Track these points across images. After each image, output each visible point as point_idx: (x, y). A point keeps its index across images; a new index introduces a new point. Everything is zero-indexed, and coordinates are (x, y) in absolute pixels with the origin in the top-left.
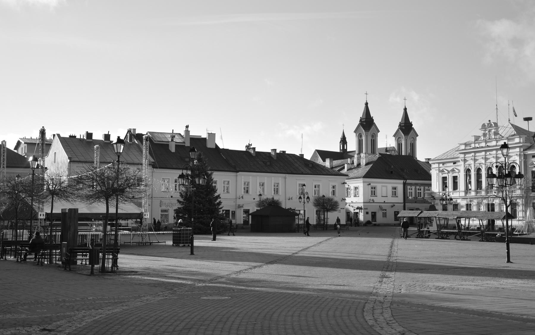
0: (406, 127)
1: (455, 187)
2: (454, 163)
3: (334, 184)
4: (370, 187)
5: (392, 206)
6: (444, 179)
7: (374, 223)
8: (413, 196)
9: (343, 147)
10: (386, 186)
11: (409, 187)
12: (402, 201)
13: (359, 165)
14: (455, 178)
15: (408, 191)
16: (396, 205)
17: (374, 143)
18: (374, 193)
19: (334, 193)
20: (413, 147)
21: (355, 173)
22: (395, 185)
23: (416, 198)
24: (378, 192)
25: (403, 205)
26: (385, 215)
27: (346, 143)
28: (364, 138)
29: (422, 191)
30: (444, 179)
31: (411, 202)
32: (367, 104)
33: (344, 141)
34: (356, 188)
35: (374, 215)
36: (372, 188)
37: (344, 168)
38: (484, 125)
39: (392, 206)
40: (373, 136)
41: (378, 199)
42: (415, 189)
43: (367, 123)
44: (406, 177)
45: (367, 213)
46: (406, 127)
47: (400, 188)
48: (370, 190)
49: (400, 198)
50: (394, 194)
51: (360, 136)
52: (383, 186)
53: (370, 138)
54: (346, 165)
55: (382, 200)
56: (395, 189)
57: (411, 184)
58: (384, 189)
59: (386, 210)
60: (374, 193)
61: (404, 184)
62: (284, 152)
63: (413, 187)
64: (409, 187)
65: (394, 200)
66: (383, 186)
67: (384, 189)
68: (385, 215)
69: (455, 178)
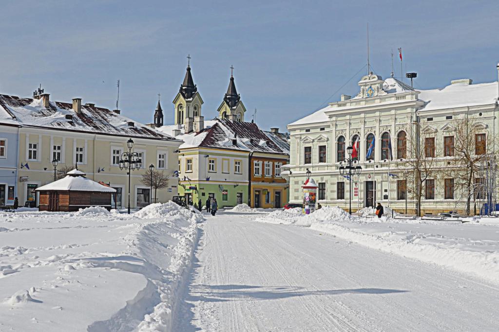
0: (233, 99)
1: (322, 159)
6: (308, 150)
11: (255, 162)
14: (322, 149)
15: (255, 167)
16: (240, 184)
19: (161, 164)
24: (218, 166)
25: (248, 184)
27: (162, 116)
29: (271, 168)
30: (308, 150)
31: (257, 180)
34: (189, 161)
36: (210, 162)
39: (235, 186)
40: (195, 108)
42: (263, 164)
43: (189, 90)
46: (233, 99)
48: (208, 164)
55: (222, 178)
57: (258, 158)
59: (227, 191)
63: (261, 162)
65: (237, 178)
66: (223, 159)
67: (226, 162)
69: (322, 149)
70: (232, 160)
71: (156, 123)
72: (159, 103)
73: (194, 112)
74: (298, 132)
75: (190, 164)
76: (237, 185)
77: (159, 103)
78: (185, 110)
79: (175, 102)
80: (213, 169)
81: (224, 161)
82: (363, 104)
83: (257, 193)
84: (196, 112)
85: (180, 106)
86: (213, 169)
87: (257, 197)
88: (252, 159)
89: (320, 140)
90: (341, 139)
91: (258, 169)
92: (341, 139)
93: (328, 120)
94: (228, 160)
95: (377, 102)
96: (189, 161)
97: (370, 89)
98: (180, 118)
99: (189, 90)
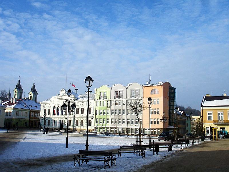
1: (49, 113)
6: (45, 110)
8: (33, 116)
10: (23, 112)
12: (29, 118)
13: (12, 103)
14: (49, 110)
23: (34, 117)
39: (24, 120)
40: (20, 93)
41: (19, 117)
49: (28, 117)
50: (26, 115)
58: (22, 113)
65: (26, 118)
69: (49, 110)
78: (17, 93)
79: (14, 90)
81: (21, 113)
90: (54, 107)
94: (23, 112)
99: (19, 87)
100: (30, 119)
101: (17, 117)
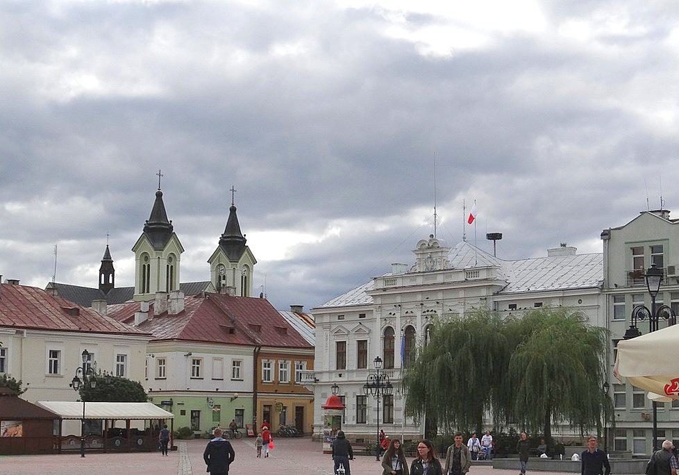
2: (362, 316)
3: (122, 352)
4: (190, 360)
5: (232, 399)
6: (341, 346)
7: (196, 432)
8: (272, 378)
9: (107, 279)
13: (164, 314)
14: (362, 344)
15: (263, 369)
17: (171, 272)
18: (196, 374)
19: (121, 369)
20: (245, 280)
21: (158, 330)
22: (237, 357)
23: (276, 383)
26: (217, 416)
27: (113, 271)
28: (153, 263)
29: (288, 369)
30: (341, 346)
32: (159, 195)
33: (107, 268)
35: (195, 415)
37: (133, 318)
38: (422, 243)
39: (232, 399)
40: (170, 259)
42: (276, 364)
44: (259, 341)
45: (183, 413)
47: (248, 361)
49: (247, 385)
51: (146, 257)
52: (215, 359)
53: (164, 263)
54: (137, 315)
56: (238, 363)
58: (217, 363)
59: (219, 406)
60: (196, 374)
61: (256, 356)
62: (15, 282)
63: (273, 363)
64: (263, 361)
65: (236, 387)
66: (215, 359)
68: (217, 416)
69: (362, 344)
70: (228, 360)
71: (103, 282)
72: (108, 248)
73: (168, 266)
74: (326, 319)
75: (162, 366)
76: (236, 398)
77: (108, 248)
80: (198, 375)
82: (420, 281)
83: (267, 409)
84: (172, 266)
85: (146, 257)
86: (198, 375)
87: (267, 416)
88: (259, 357)
89: (358, 331)
91: (269, 371)
92: (388, 332)
93: (370, 300)
94: (220, 359)
95: (440, 279)
96: (162, 362)
97: (430, 260)
98: (144, 277)
100: (255, 392)
101: (196, 385)
